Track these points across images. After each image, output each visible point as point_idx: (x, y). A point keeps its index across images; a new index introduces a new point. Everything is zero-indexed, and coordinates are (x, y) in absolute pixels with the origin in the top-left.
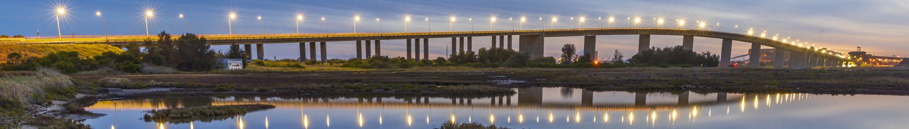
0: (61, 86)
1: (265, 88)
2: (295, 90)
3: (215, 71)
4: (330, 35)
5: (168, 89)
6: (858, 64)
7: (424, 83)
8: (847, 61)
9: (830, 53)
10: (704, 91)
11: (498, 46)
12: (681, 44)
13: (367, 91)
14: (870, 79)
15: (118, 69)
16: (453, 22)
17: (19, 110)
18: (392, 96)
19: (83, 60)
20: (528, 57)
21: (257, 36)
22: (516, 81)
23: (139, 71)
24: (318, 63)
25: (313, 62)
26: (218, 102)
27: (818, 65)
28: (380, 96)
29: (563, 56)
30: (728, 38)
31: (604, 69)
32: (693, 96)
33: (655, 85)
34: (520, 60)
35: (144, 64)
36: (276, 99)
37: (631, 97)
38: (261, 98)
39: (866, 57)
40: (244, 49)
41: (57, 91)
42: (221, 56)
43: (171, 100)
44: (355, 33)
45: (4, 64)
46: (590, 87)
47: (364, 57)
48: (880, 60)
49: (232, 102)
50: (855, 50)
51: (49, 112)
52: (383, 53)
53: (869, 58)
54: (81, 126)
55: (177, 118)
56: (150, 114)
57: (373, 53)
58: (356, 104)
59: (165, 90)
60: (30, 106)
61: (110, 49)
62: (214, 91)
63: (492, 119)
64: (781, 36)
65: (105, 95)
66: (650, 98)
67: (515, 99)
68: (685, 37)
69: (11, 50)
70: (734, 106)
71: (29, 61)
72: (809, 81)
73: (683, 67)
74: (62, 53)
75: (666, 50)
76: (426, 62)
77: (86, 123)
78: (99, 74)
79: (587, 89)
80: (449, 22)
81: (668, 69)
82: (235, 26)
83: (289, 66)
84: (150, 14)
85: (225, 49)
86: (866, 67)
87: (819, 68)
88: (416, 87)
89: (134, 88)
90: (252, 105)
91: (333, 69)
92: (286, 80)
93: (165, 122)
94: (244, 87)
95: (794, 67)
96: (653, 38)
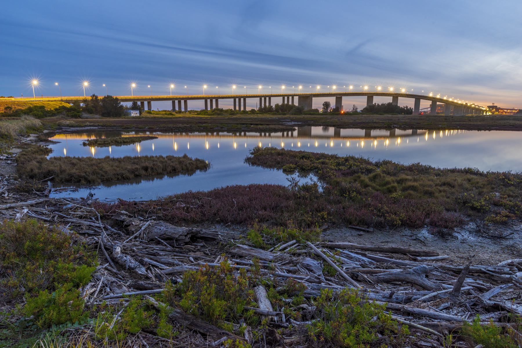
0: (35, 126)
1: (152, 127)
2: (169, 128)
3: (123, 117)
4: (190, 96)
5: (97, 128)
6: (493, 113)
7: (243, 124)
8: (486, 111)
9: (477, 107)
10: (404, 129)
11: (286, 102)
12: (391, 102)
13: (211, 128)
14: (499, 122)
15: (68, 116)
16: (260, 89)
17: (11, 139)
18: (225, 131)
19: (48, 111)
20: (303, 109)
21: (148, 97)
22: (296, 123)
23: (80, 117)
24: (183, 112)
25: (180, 112)
26: (125, 135)
27: (470, 114)
28: (218, 131)
29: (324, 108)
30: (418, 98)
31: (347, 116)
32: (398, 131)
33: (376, 125)
34: (299, 110)
35: (83, 113)
36: (159, 133)
37: (362, 132)
38: (150, 133)
39: (497, 109)
40: (140, 104)
41: (33, 129)
42: (127, 108)
43: (98, 134)
44: (204, 95)
45: (2, 113)
46: (339, 126)
47: (209, 109)
48: (505, 111)
49: (133, 135)
50: (491, 105)
51: (28, 141)
52: (220, 107)
53: (499, 110)
54: (47, 148)
55: (102, 144)
56: (86, 142)
57: (214, 107)
58: (204, 136)
59: (95, 128)
60: (17, 137)
61: (63, 104)
62: (123, 129)
63: (283, 145)
64: (449, 97)
65: (61, 131)
66: (373, 133)
67: (295, 133)
68: (393, 97)
69: (6, 105)
70: (422, 137)
71: (17, 111)
72: (465, 123)
73: (392, 114)
74: (36, 107)
75: (383, 105)
76: (245, 112)
77: (49, 147)
78: (57, 119)
79: (337, 128)
80: (258, 88)
81: (384, 116)
82: (135, 91)
83: (166, 114)
84: (86, 84)
85: (129, 104)
86: (497, 115)
87: (470, 115)
88: (239, 126)
89: (77, 127)
90: (145, 137)
91: (191, 116)
92: (164, 122)
93: (95, 146)
94: (140, 126)
95: (456, 115)
96: (375, 98)
